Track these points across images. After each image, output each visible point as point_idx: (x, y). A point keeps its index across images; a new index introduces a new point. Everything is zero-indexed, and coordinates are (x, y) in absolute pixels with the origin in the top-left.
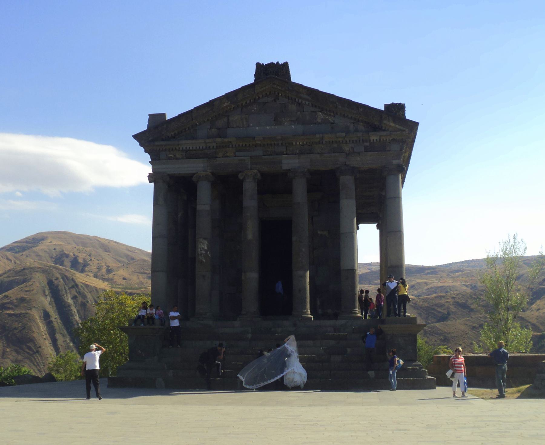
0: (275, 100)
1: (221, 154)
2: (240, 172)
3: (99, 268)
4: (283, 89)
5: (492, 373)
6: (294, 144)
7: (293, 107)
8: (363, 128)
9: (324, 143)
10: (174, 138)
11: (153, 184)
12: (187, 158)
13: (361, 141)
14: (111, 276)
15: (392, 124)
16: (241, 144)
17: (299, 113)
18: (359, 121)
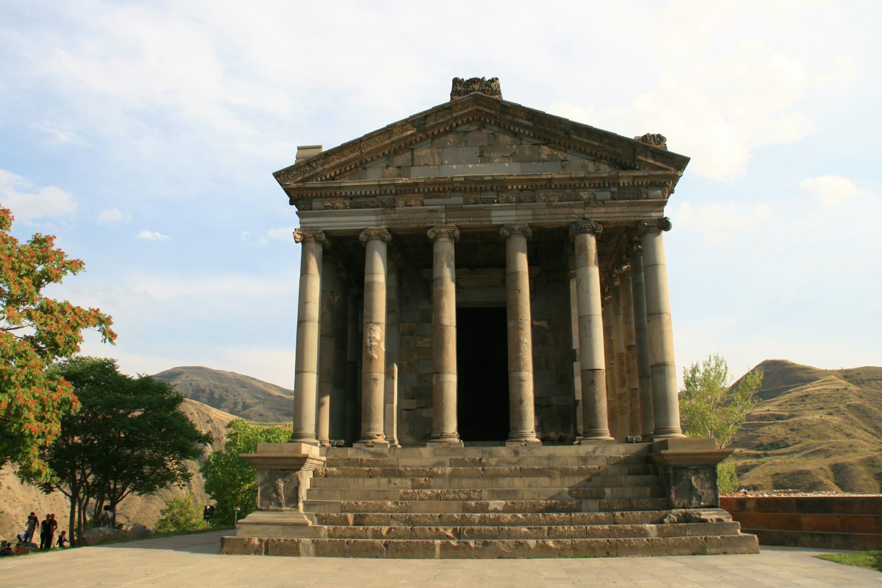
0: (479, 129)
1: (401, 202)
2: (430, 228)
3: (236, 404)
4: (493, 112)
5: (784, 523)
6: (510, 187)
7: (505, 139)
8: (607, 167)
9: (553, 186)
10: (333, 179)
11: (300, 244)
12: (352, 207)
13: (607, 185)
14: (247, 412)
15: (651, 161)
16: (431, 189)
17: (514, 147)
18: (601, 158)
